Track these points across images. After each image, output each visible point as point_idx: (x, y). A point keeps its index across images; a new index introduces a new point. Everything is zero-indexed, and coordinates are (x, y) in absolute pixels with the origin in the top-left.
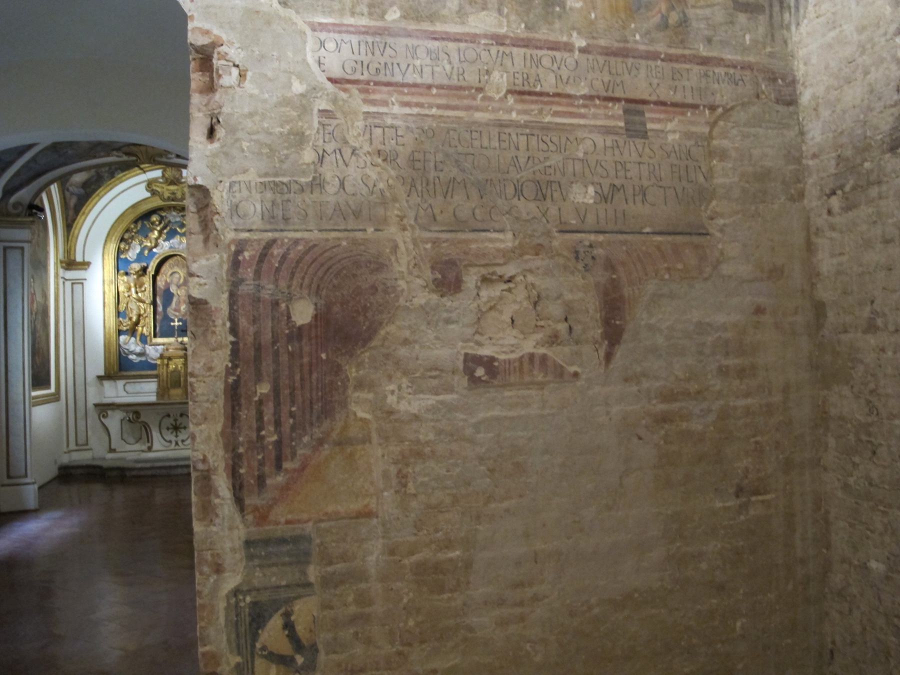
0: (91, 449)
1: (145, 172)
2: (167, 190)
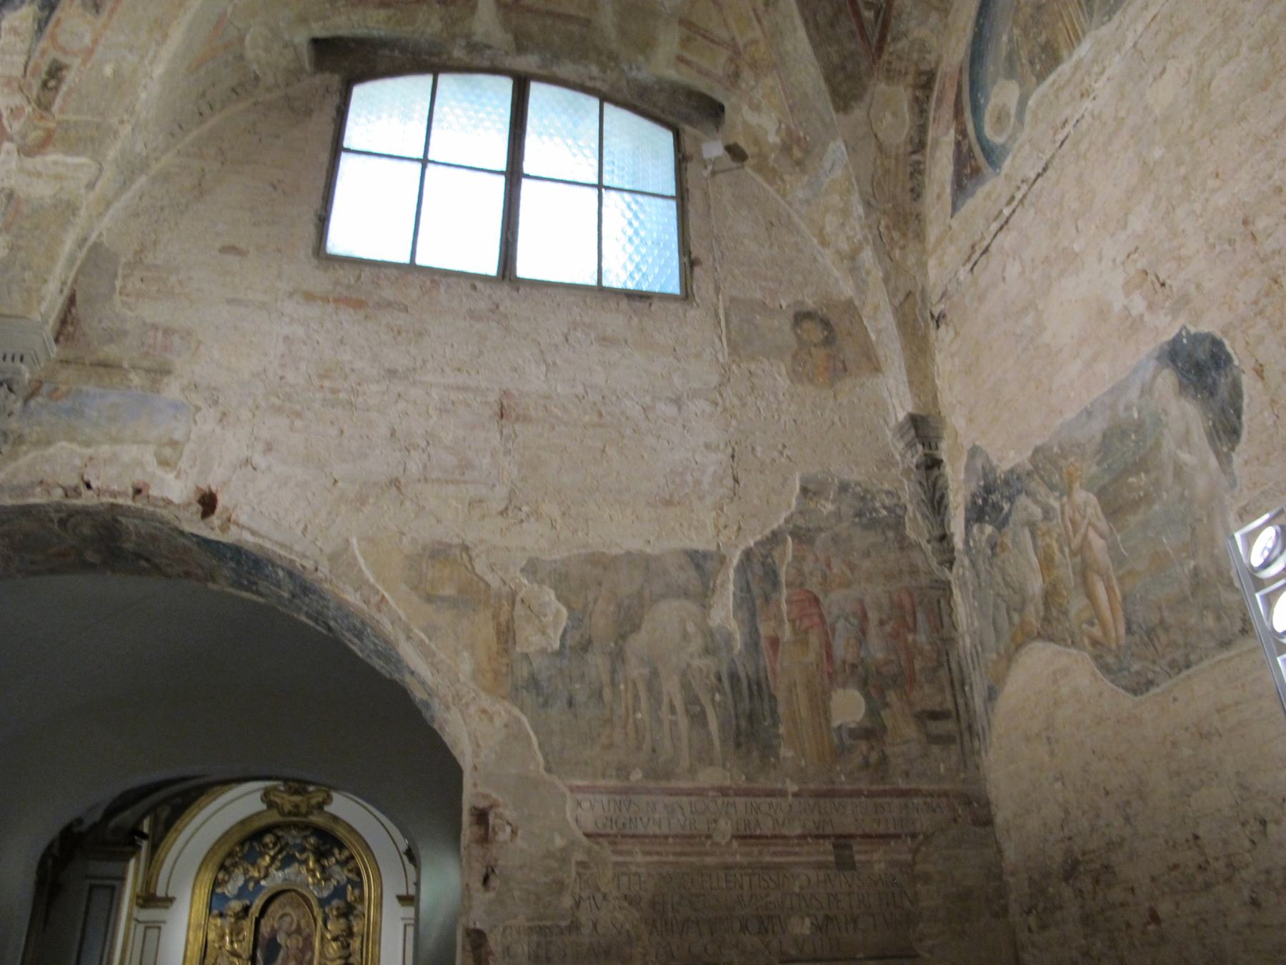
2: (288, 801)
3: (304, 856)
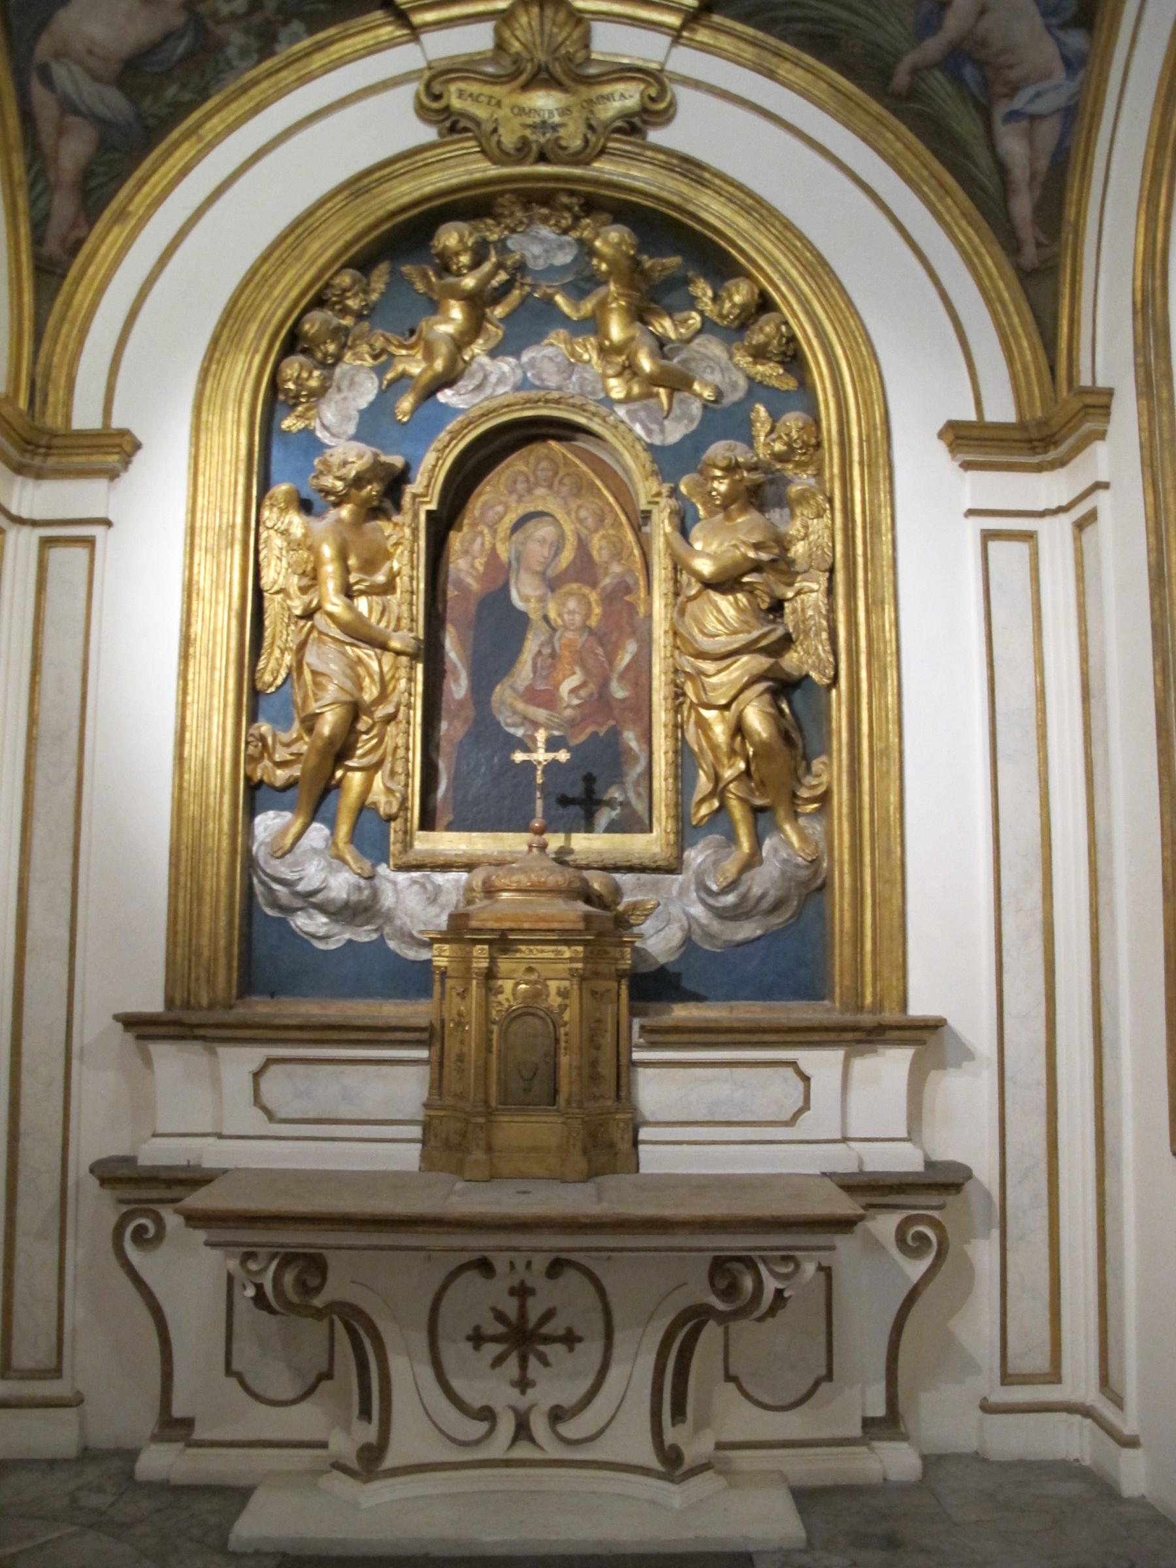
1: (415, 33)
3: (588, 306)
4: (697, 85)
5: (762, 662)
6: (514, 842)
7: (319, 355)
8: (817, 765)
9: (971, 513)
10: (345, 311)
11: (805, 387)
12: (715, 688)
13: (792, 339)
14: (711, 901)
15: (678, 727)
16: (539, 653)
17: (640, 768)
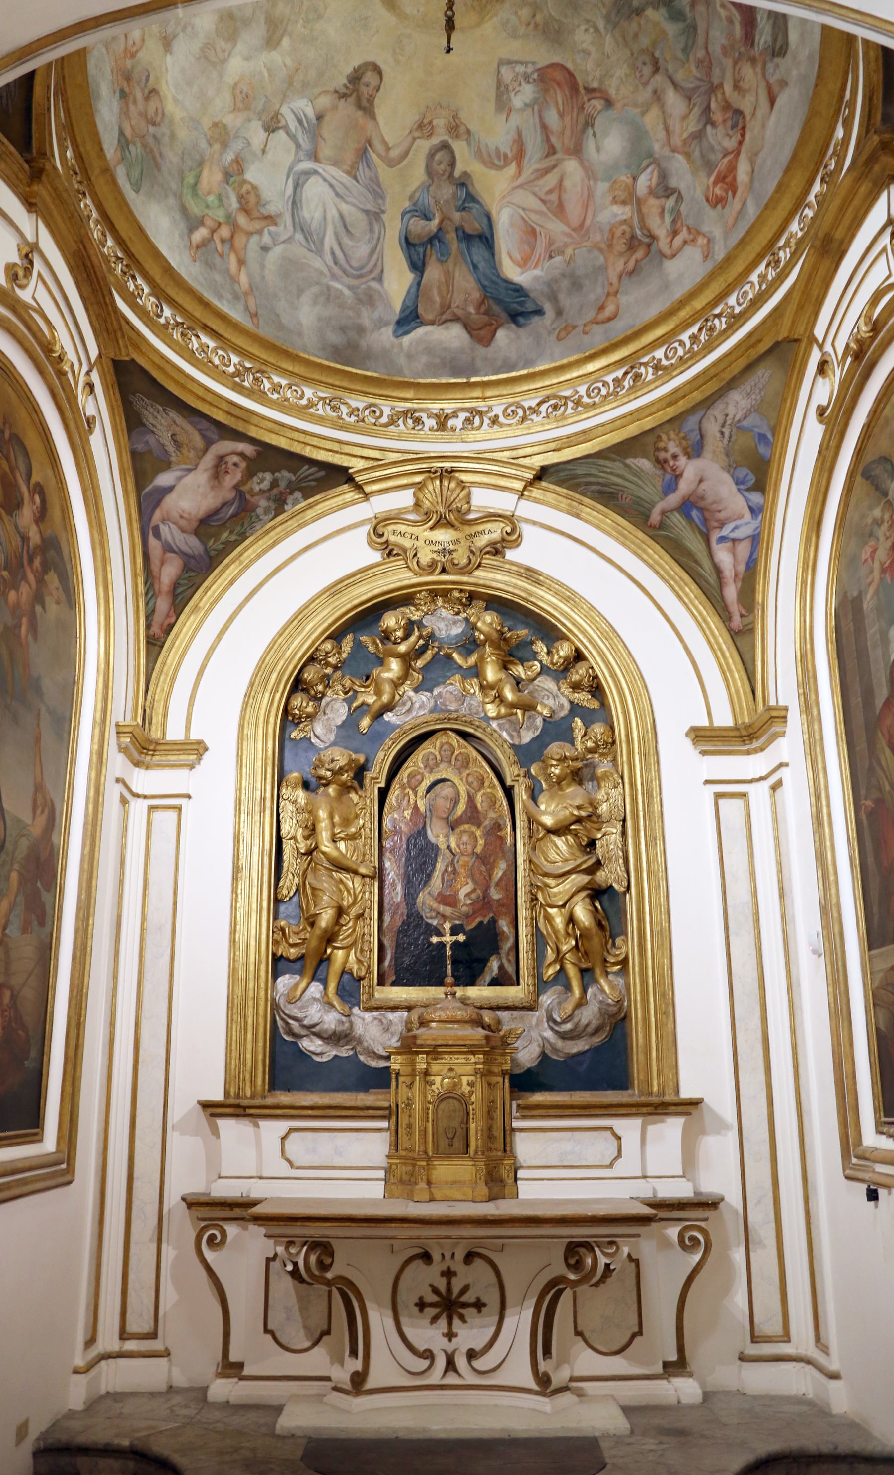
0: (167, 1354)
1: (367, 496)
2: (430, 541)
3: (472, 660)
4: (534, 523)
5: (584, 879)
6: (436, 992)
7: (313, 692)
8: (619, 941)
9: (707, 782)
10: (328, 664)
11: (604, 705)
12: (555, 895)
13: (596, 677)
14: (556, 1028)
15: (534, 920)
16: (446, 870)
17: (510, 943)
